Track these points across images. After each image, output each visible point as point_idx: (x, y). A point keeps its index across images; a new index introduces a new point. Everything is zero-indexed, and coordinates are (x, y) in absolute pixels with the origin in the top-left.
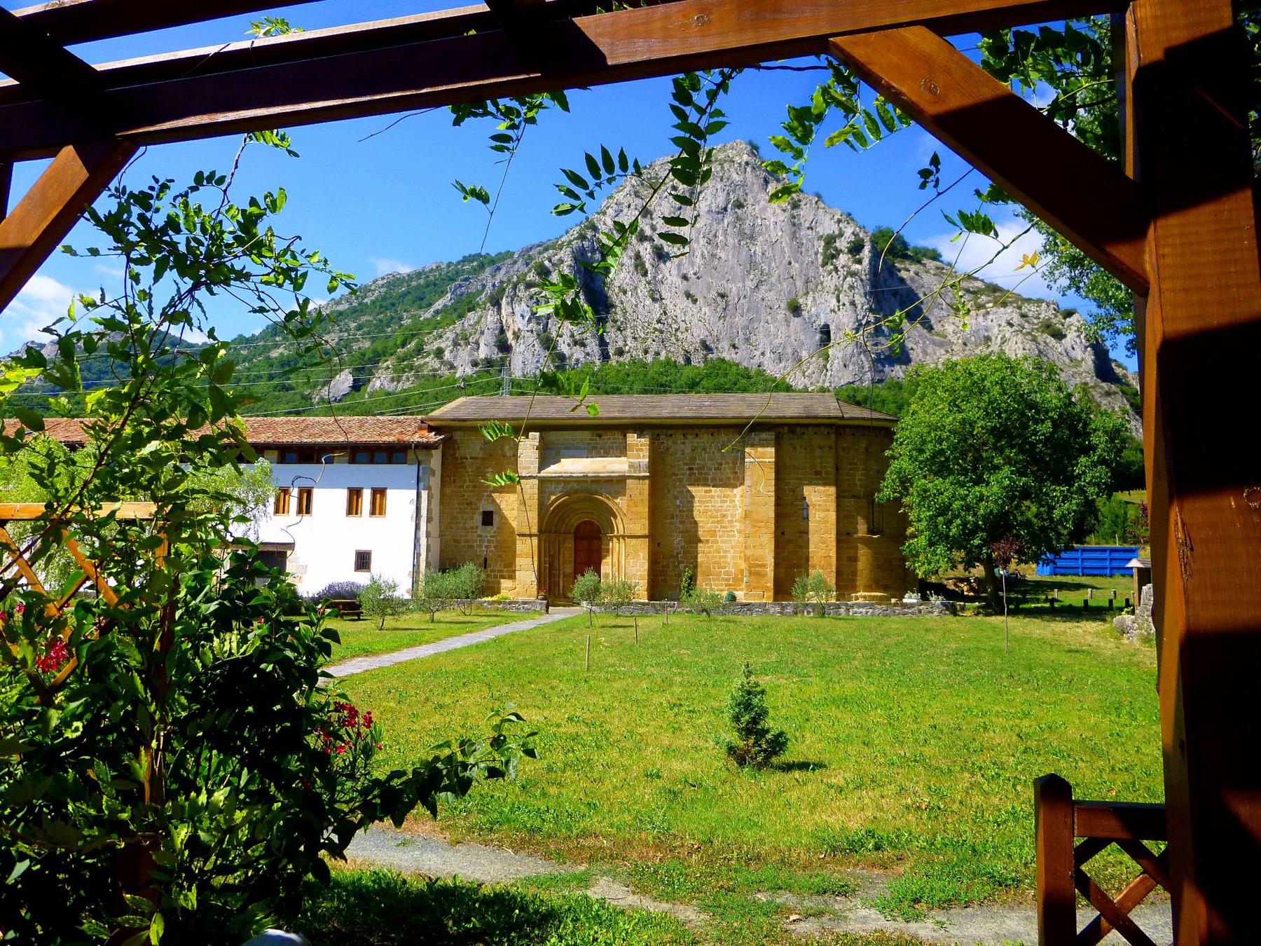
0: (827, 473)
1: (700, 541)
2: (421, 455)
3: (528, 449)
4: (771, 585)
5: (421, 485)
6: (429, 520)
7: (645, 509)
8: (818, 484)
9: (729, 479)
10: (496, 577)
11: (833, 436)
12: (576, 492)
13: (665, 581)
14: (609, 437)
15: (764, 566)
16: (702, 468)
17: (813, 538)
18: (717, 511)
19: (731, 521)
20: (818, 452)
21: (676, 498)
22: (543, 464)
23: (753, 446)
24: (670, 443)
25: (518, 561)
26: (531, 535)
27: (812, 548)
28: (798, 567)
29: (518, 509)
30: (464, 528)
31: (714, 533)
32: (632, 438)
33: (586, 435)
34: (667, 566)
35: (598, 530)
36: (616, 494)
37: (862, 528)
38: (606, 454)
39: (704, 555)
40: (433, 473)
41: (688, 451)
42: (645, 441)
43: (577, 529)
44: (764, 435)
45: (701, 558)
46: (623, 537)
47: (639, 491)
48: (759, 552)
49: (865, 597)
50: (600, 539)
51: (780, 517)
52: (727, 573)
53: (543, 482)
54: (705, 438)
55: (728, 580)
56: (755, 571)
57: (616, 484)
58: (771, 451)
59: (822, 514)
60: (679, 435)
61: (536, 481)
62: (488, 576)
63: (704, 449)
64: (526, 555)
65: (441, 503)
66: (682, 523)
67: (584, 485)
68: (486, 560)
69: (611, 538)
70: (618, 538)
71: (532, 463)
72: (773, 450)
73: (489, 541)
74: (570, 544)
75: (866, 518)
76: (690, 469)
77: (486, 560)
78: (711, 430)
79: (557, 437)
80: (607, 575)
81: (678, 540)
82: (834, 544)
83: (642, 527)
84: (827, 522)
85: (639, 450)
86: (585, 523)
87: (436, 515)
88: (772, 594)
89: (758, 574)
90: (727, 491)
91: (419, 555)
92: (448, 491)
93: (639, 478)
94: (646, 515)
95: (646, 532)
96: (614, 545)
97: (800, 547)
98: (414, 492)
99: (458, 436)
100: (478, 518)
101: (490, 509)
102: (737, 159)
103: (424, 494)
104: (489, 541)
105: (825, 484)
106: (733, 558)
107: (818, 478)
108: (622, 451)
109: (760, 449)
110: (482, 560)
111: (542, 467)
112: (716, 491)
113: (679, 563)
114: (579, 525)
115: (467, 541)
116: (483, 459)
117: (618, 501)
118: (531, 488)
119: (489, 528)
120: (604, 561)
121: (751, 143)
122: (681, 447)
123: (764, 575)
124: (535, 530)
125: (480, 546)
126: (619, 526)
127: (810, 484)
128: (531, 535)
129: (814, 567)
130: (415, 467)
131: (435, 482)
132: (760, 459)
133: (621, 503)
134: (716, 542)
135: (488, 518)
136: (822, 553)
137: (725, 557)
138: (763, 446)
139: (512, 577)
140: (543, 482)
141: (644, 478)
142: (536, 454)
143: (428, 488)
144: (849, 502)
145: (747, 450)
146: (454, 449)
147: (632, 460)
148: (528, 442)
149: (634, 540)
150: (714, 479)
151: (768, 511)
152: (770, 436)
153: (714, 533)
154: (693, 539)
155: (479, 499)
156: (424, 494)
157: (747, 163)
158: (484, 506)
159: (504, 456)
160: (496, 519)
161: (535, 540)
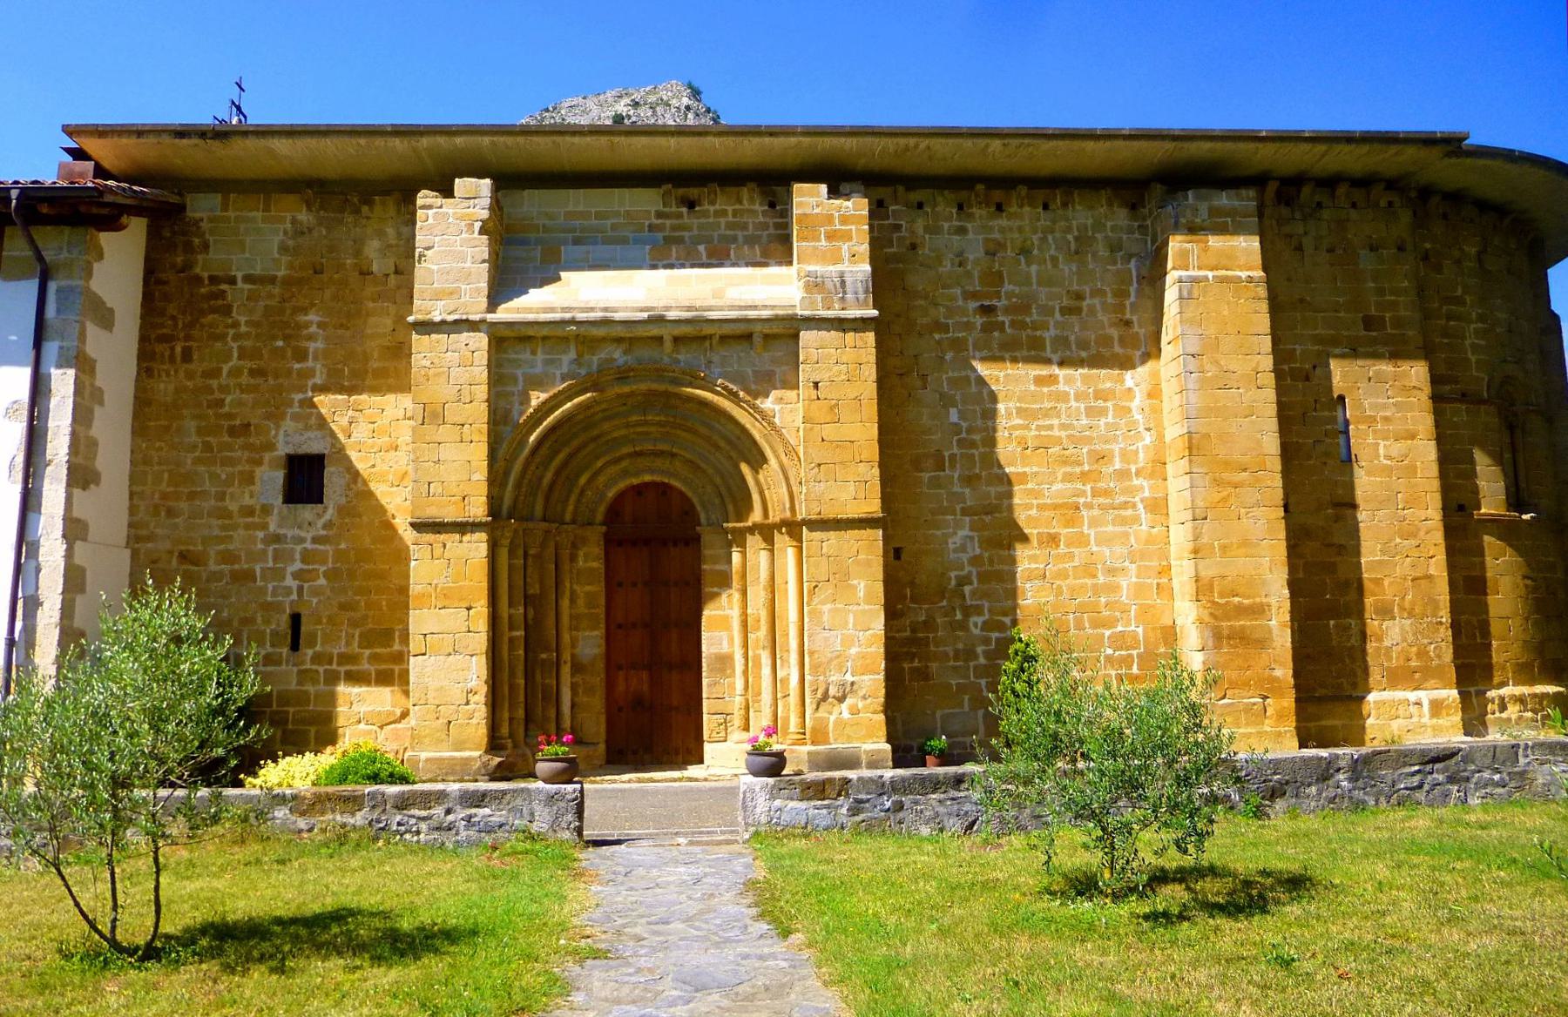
0: (1398, 323)
1: (1025, 539)
2: (54, 243)
3: (450, 238)
4: (1284, 672)
5: (51, 349)
6: (81, 476)
7: (864, 431)
8: (1376, 356)
9: (1106, 341)
10: (333, 679)
11: (1405, 217)
12: (623, 376)
13: (924, 675)
14: (720, 209)
15: (1259, 610)
16: (1024, 308)
17: (1372, 523)
18: (1077, 441)
19: (1123, 474)
20: (1366, 261)
21: (947, 401)
22: (503, 284)
23: (1192, 230)
24: (920, 225)
25: (420, 621)
26: (462, 528)
27: (1370, 554)
28: (1335, 611)
29: (415, 448)
30: (225, 514)
31: (1070, 511)
32: (809, 199)
33: (646, 201)
34: (929, 625)
35: (688, 513)
36: (765, 382)
37: (1491, 497)
38: (718, 258)
39: (1040, 584)
40: (105, 318)
41: (975, 254)
42: (856, 207)
43: (614, 512)
44: (1224, 199)
45: (1031, 596)
46: (793, 528)
47: (842, 368)
48: (1240, 565)
49: (1521, 700)
50: (693, 541)
51: (1289, 453)
52: (1120, 641)
53: (508, 343)
54: (1021, 220)
55: (1127, 662)
56: (1230, 628)
57: (768, 344)
58: (1249, 245)
59: (1397, 448)
60: (944, 206)
61: (480, 340)
62: (304, 675)
63: (1025, 251)
64: (446, 598)
65: (140, 427)
66: (969, 480)
67: (645, 353)
68: (296, 619)
69: (739, 538)
70: (767, 532)
71: (467, 277)
72: (1254, 243)
73: (306, 557)
74: (591, 558)
75: (1498, 459)
76: (987, 310)
77: (296, 619)
78: (1041, 195)
79: (550, 193)
80: (724, 661)
81: (959, 540)
82: (1439, 536)
83: (858, 491)
84: (1412, 470)
85: (833, 244)
86: (639, 490)
87: (114, 459)
88: (1289, 702)
89: (1241, 639)
90: (1105, 377)
91: (33, 604)
92: (164, 388)
93: (841, 325)
94: (873, 452)
95: (872, 506)
96: (752, 559)
97: (1341, 549)
98: (26, 373)
99: (201, 207)
100: (272, 479)
101: (314, 446)
102: (674, 102)
103: (63, 382)
104: (306, 557)
105: (1396, 355)
106: (1139, 589)
107: (1378, 340)
108: (775, 245)
109: (1215, 241)
110: (284, 621)
111: (500, 290)
112: (1071, 380)
113: (967, 612)
114: (621, 496)
115: (229, 557)
116: (288, 282)
117: (767, 404)
118: (455, 369)
119: (307, 512)
120: (708, 613)
121: (690, 86)
122: (956, 241)
123: (1262, 643)
124: (478, 509)
125: (279, 574)
126: (771, 490)
127: (1353, 352)
128: (462, 528)
129: (1385, 612)
130: (31, 287)
131: (115, 351)
132: (1214, 279)
133: (782, 413)
134: (1082, 541)
135: (306, 477)
136: (1403, 568)
137: (1114, 588)
138: (1222, 230)
139: (392, 673)
140: (508, 343)
141: (859, 325)
142: (481, 247)
143: (83, 365)
144: (1459, 413)
145: (1176, 244)
146: (189, 248)
147: (824, 258)
148: (449, 207)
149: (832, 541)
150: (1061, 342)
151: (1261, 435)
152: (1246, 200)
153: (1070, 511)
154: (1004, 535)
155: (276, 417)
156: (63, 382)
157: (688, 108)
158: (289, 439)
159: (365, 273)
160: (332, 479)
161: (476, 547)
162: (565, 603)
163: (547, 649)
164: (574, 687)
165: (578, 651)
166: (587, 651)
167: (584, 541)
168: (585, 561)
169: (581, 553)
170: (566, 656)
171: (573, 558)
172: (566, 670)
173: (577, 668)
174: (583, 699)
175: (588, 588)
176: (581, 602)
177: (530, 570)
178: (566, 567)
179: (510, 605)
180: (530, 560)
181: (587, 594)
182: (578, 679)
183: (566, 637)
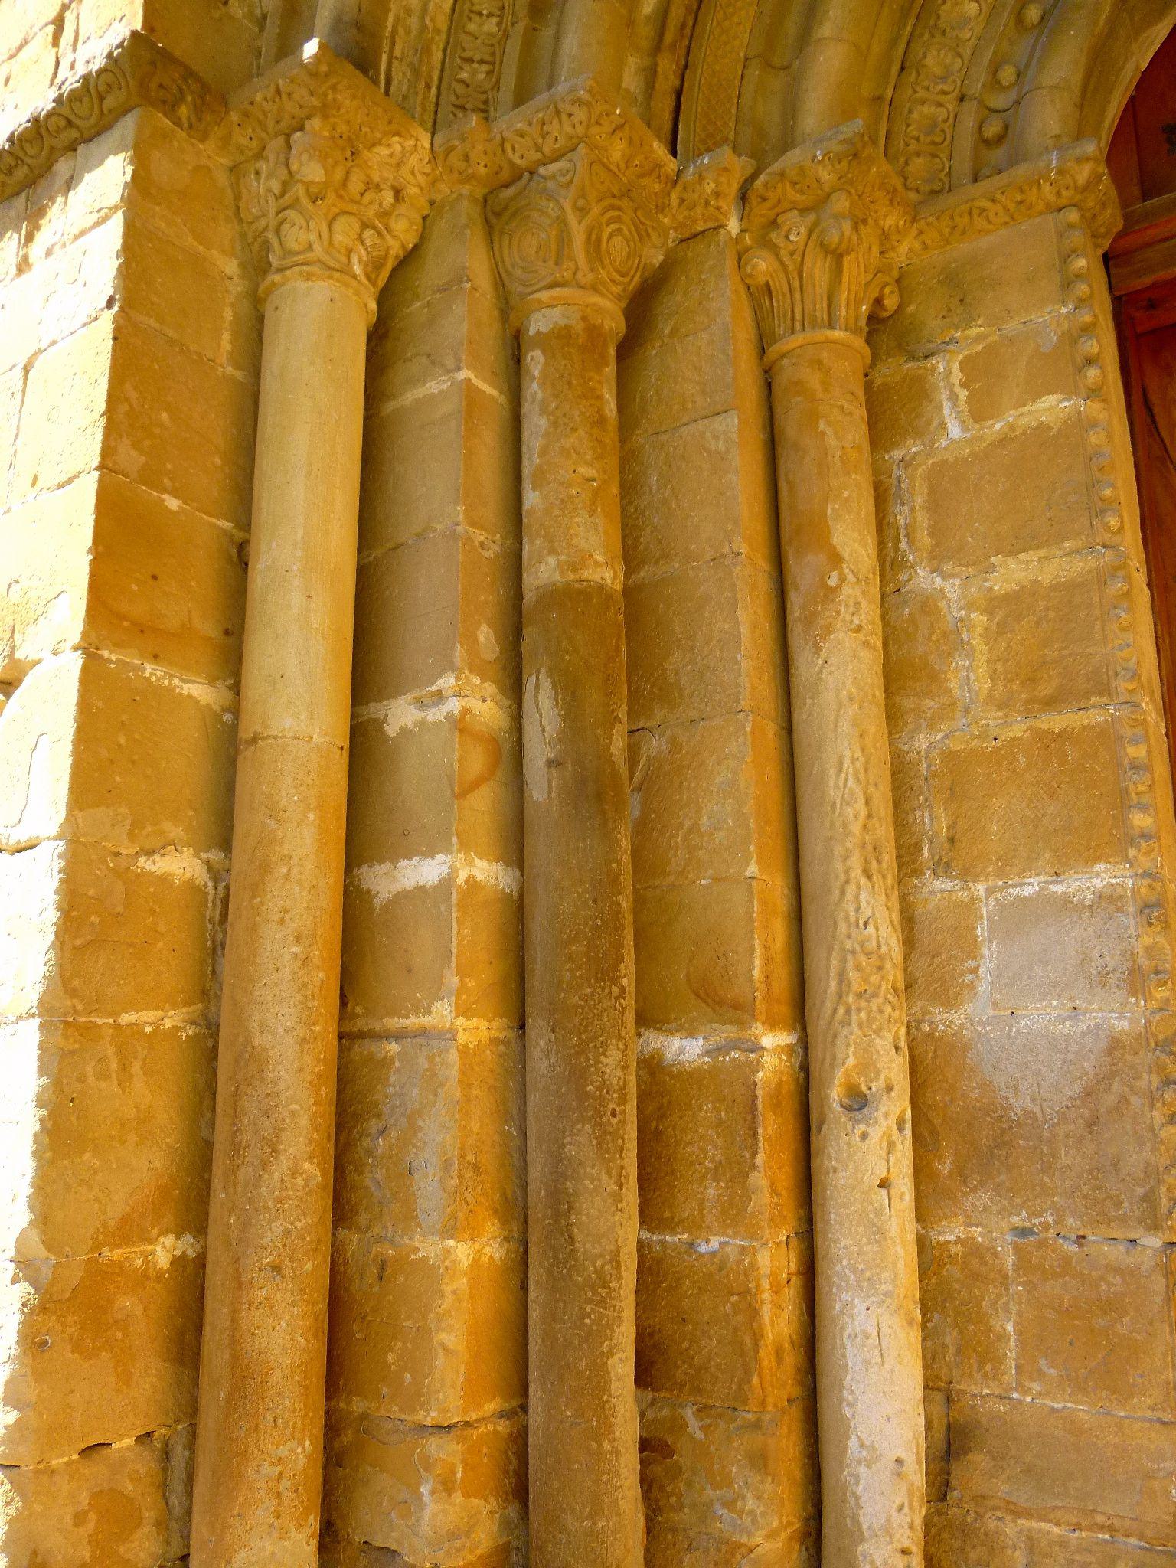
162: (843, 669)
163: (717, 1001)
164: (944, 1294)
165: (970, 1016)
166: (1040, 1017)
167: (961, 290)
168: (979, 411)
169: (947, 371)
170: (870, 1051)
171: (888, 415)
172: (871, 1159)
173: (956, 1133)
174: (1022, 1394)
175: (1012, 572)
176: (970, 674)
177: (536, 425)
178: (837, 430)
179: (369, 671)
180: (535, 361)
181: (1009, 608)
182: (979, 1224)
183: (863, 915)
